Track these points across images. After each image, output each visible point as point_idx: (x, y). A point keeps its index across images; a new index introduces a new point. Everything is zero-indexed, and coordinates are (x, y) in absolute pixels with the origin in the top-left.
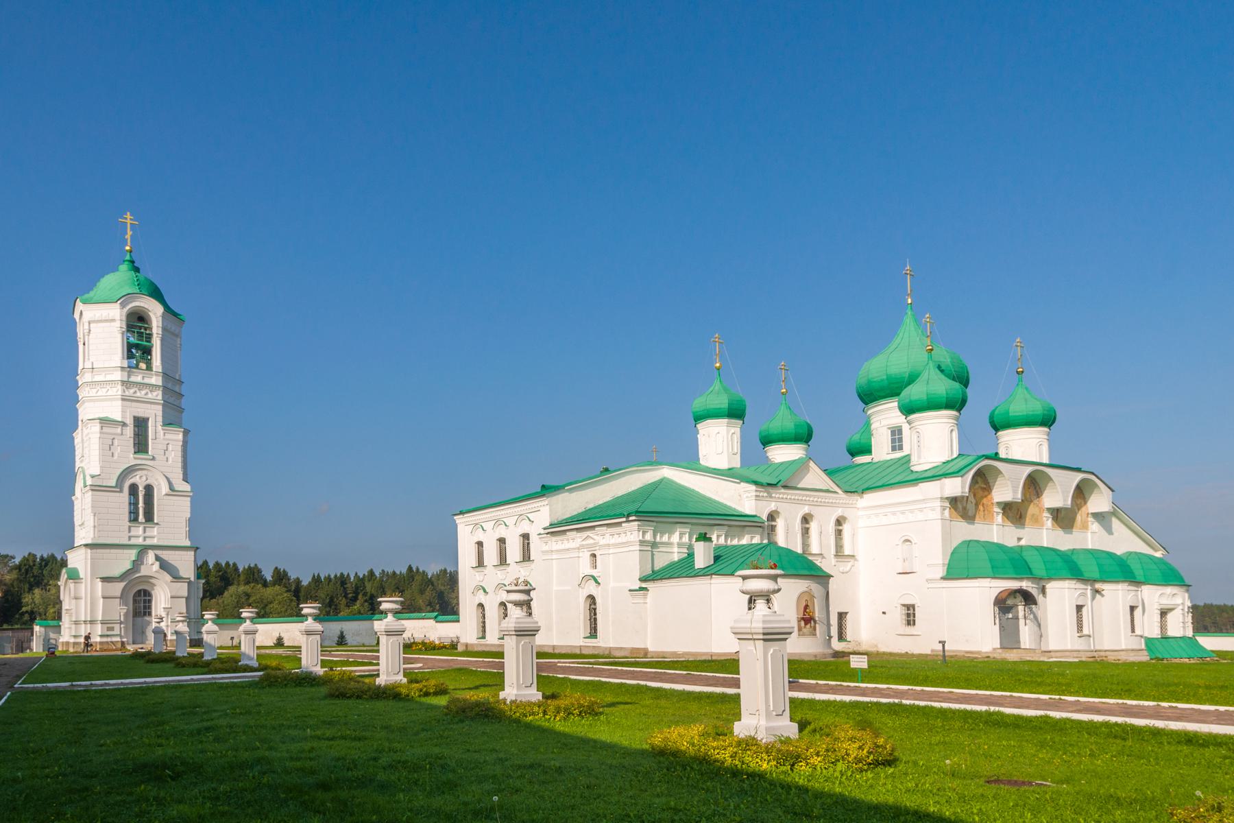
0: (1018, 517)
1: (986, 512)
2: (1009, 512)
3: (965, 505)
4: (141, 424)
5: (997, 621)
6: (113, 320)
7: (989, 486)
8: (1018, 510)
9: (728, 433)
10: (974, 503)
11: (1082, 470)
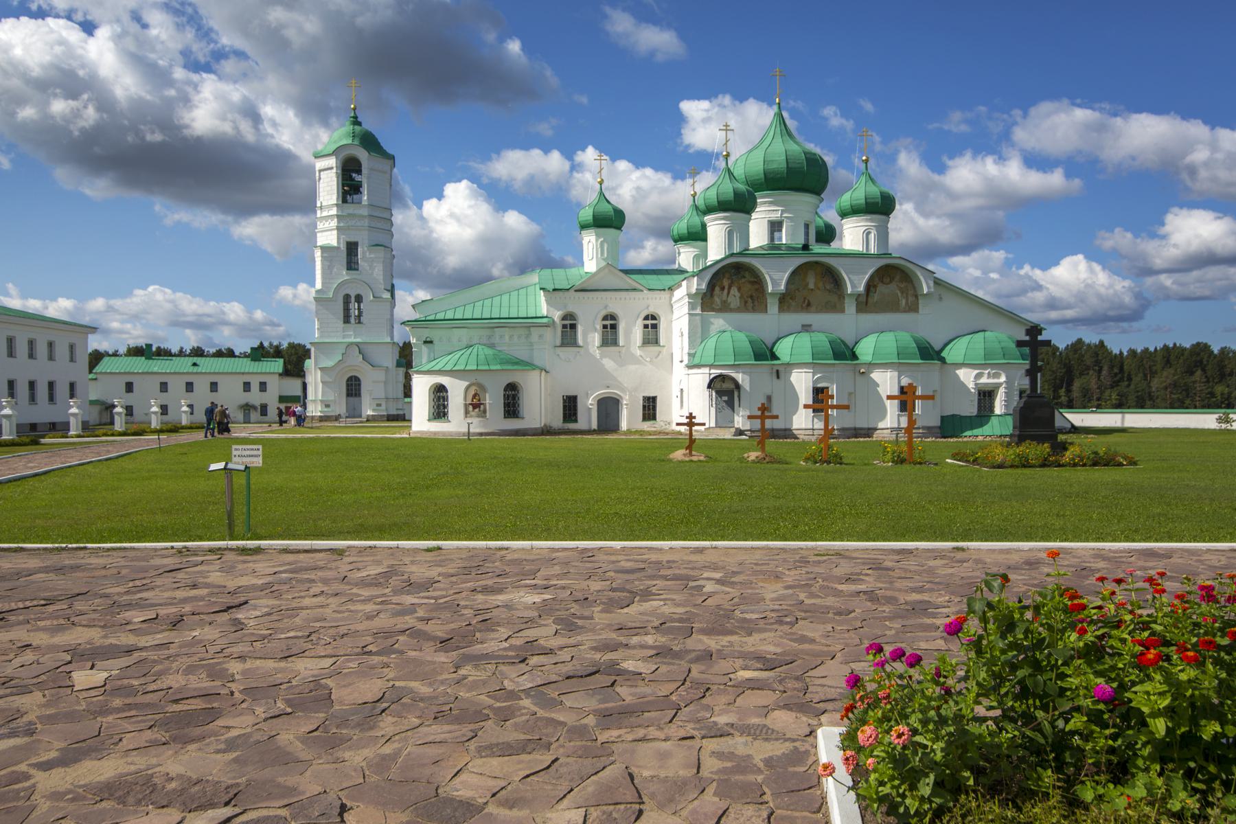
0: (804, 305)
1: (756, 303)
2: (791, 301)
3: (725, 298)
4: (352, 248)
5: (714, 405)
6: (332, 168)
7: (760, 280)
8: (805, 298)
9: (597, 241)
10: (737, 298)
11: (893, 255)
